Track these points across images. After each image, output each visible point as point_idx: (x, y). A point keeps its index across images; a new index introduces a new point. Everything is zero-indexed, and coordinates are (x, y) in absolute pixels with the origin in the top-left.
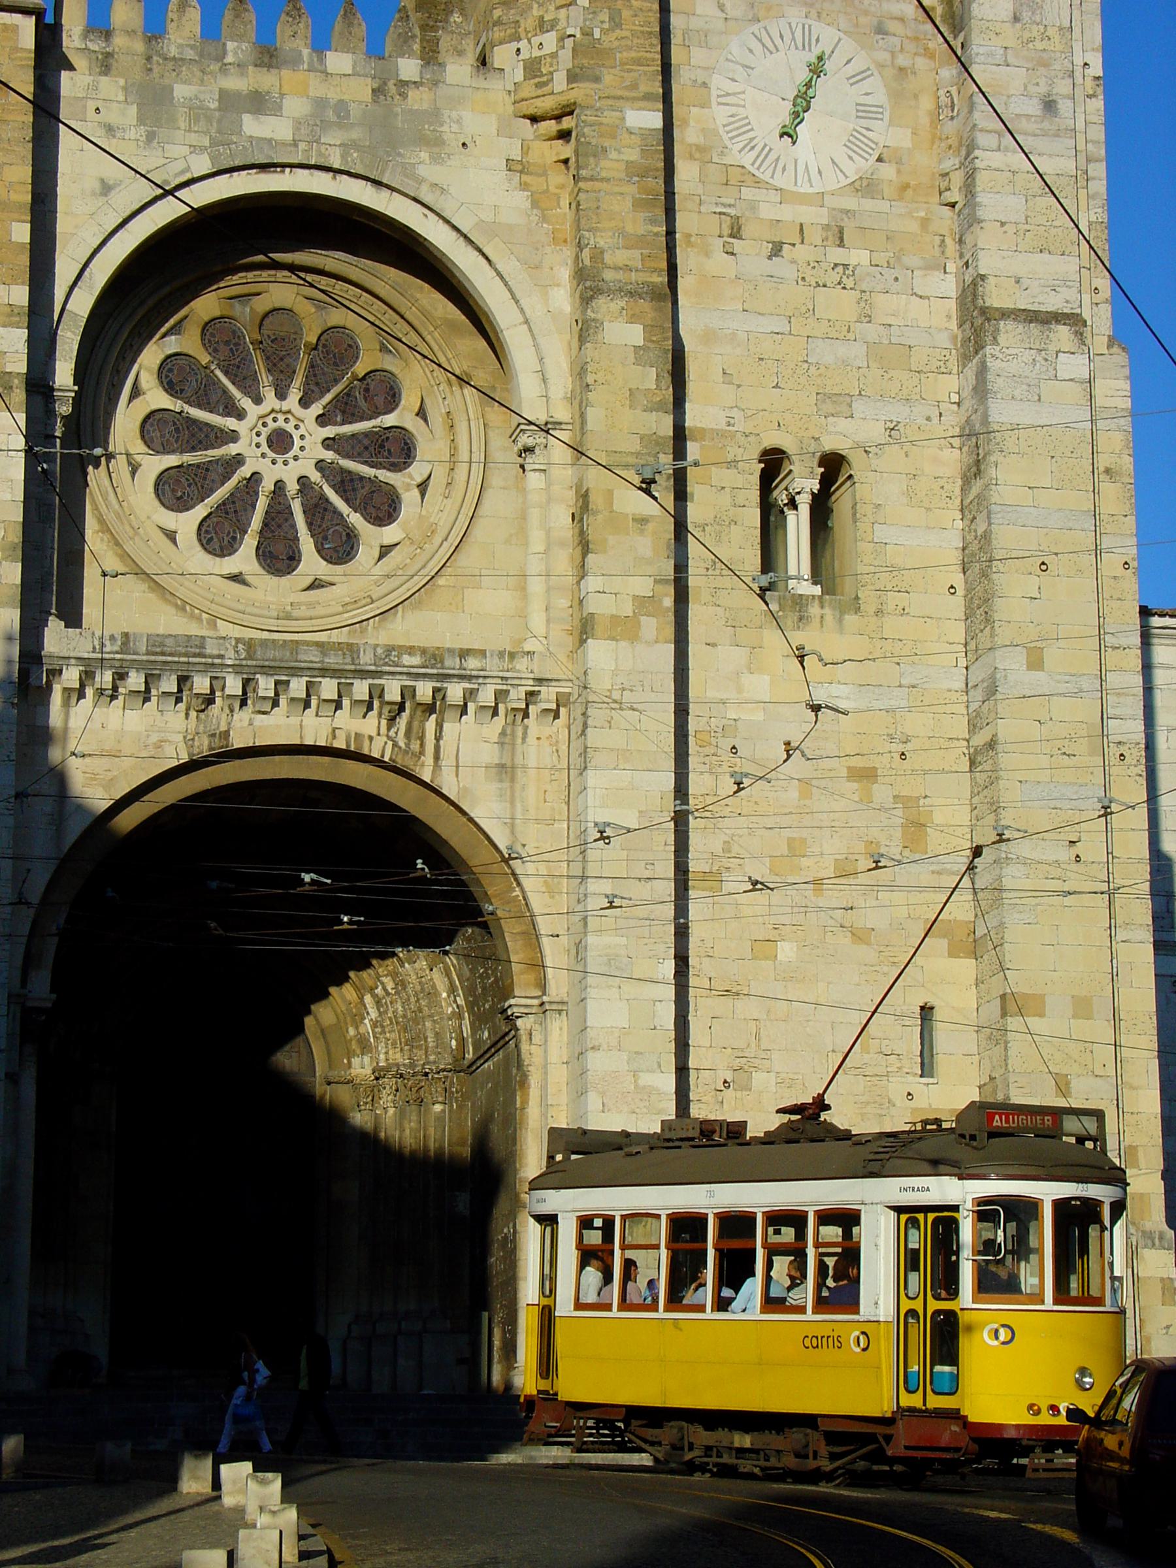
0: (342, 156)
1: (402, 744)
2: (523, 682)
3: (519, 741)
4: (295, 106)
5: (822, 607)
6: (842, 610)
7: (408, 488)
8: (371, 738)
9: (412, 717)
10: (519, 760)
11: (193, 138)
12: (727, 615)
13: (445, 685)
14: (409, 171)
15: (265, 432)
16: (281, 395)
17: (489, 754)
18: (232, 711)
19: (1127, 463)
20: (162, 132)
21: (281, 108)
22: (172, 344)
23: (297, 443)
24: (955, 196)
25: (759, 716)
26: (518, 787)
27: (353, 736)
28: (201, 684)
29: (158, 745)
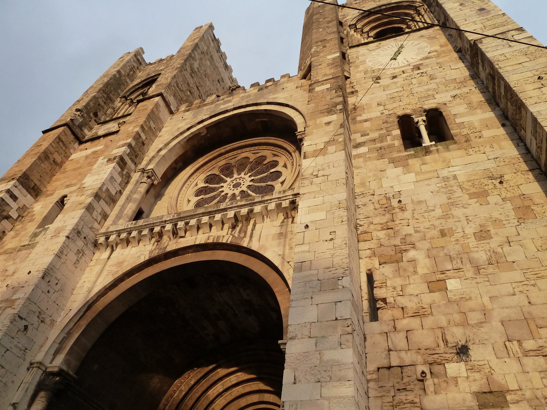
1: (236, 235)
2: (288, 198)
7: (277, 184)
8: (223, 236)
10: (289, 229)
12: (389, 160)
13: (253, 207)
15: (232, 184)
16: (239, 174)
18: (170, 239)
22: (210, 173)
23: (242, 184)
25: (412, 187)
26: (288, 240)
27: (216, 237)
28: (157, 229)
29: (139, 257)
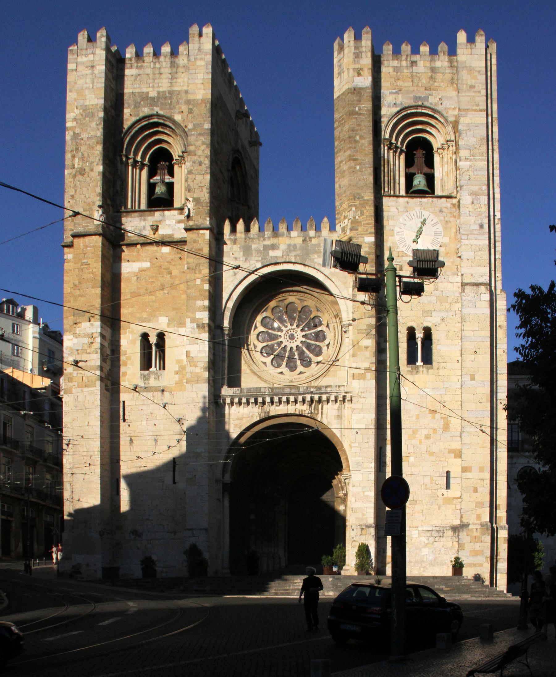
0: (295, 259)
1: (313, 411)
3: (343, 409)
4: (283, 247)
5: (423, 368)
6: (428, 369)
8: (305, 411)
9: (315, 404)
10: (343, 413)
11: (257, 258)
14: (312, 261)
17: (335, 413)
18: (270, 406)
19: (505, 324)
20: (249, 258)
21: (279, 247)
24: (459, 255)
